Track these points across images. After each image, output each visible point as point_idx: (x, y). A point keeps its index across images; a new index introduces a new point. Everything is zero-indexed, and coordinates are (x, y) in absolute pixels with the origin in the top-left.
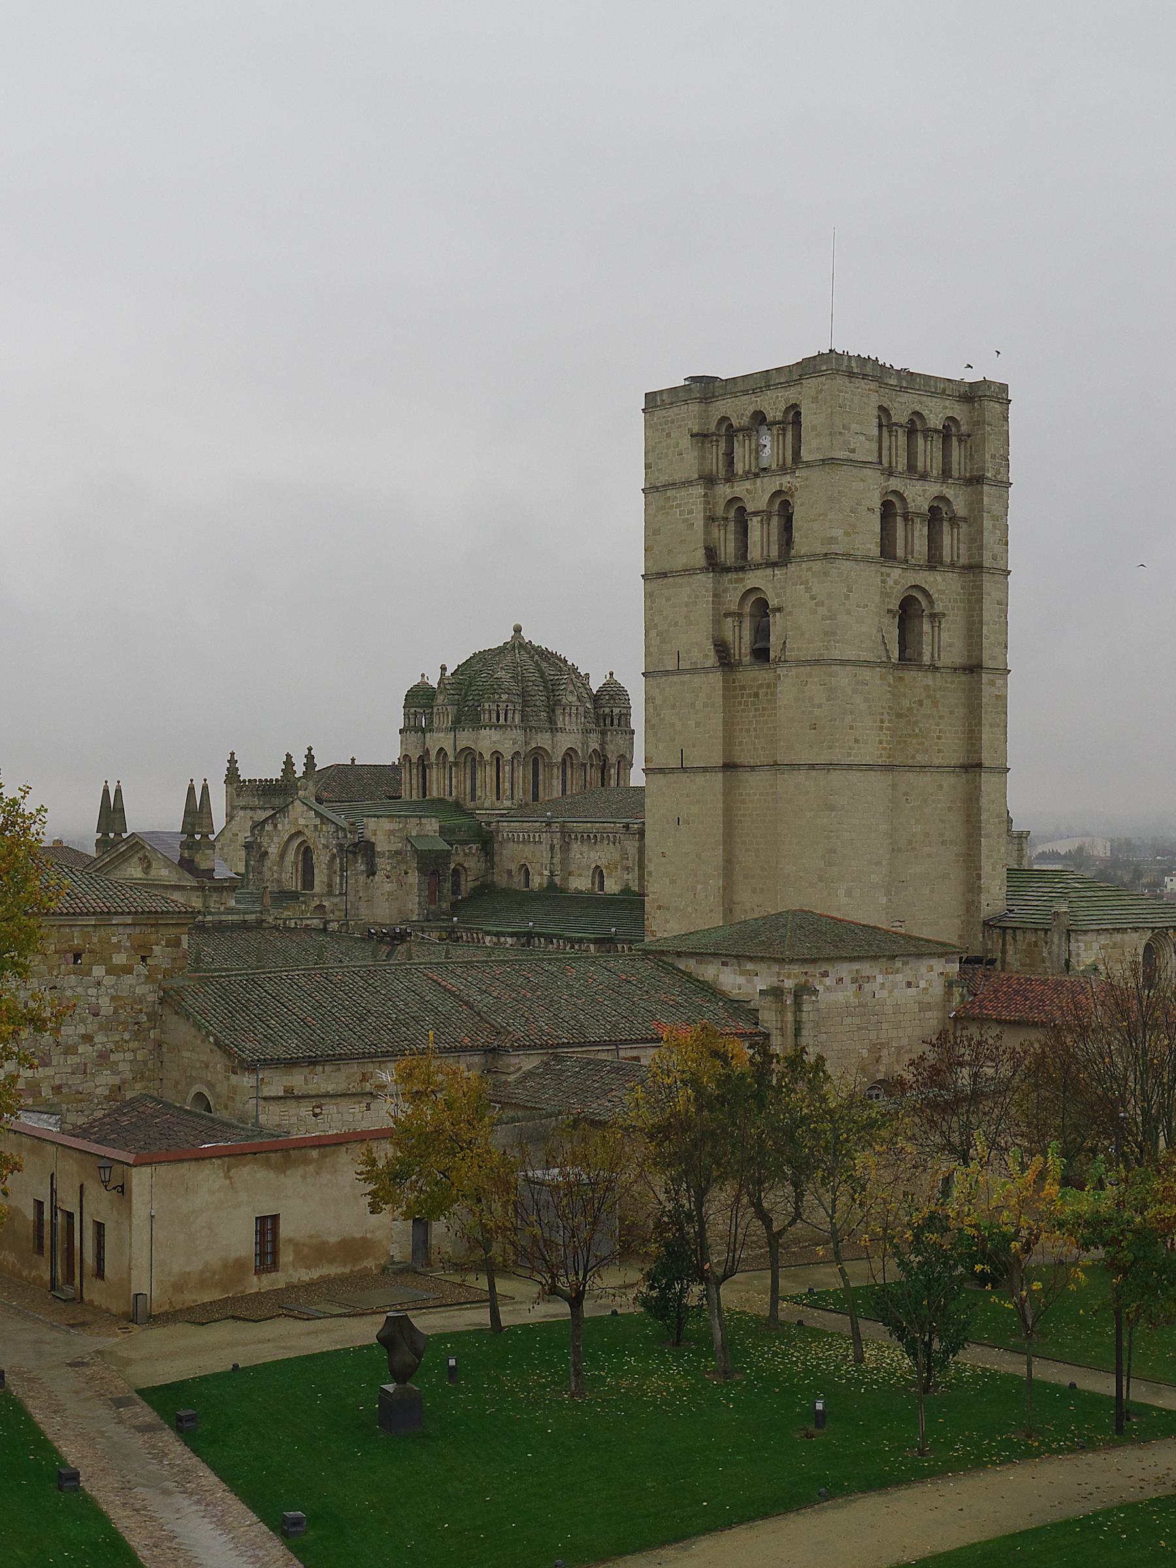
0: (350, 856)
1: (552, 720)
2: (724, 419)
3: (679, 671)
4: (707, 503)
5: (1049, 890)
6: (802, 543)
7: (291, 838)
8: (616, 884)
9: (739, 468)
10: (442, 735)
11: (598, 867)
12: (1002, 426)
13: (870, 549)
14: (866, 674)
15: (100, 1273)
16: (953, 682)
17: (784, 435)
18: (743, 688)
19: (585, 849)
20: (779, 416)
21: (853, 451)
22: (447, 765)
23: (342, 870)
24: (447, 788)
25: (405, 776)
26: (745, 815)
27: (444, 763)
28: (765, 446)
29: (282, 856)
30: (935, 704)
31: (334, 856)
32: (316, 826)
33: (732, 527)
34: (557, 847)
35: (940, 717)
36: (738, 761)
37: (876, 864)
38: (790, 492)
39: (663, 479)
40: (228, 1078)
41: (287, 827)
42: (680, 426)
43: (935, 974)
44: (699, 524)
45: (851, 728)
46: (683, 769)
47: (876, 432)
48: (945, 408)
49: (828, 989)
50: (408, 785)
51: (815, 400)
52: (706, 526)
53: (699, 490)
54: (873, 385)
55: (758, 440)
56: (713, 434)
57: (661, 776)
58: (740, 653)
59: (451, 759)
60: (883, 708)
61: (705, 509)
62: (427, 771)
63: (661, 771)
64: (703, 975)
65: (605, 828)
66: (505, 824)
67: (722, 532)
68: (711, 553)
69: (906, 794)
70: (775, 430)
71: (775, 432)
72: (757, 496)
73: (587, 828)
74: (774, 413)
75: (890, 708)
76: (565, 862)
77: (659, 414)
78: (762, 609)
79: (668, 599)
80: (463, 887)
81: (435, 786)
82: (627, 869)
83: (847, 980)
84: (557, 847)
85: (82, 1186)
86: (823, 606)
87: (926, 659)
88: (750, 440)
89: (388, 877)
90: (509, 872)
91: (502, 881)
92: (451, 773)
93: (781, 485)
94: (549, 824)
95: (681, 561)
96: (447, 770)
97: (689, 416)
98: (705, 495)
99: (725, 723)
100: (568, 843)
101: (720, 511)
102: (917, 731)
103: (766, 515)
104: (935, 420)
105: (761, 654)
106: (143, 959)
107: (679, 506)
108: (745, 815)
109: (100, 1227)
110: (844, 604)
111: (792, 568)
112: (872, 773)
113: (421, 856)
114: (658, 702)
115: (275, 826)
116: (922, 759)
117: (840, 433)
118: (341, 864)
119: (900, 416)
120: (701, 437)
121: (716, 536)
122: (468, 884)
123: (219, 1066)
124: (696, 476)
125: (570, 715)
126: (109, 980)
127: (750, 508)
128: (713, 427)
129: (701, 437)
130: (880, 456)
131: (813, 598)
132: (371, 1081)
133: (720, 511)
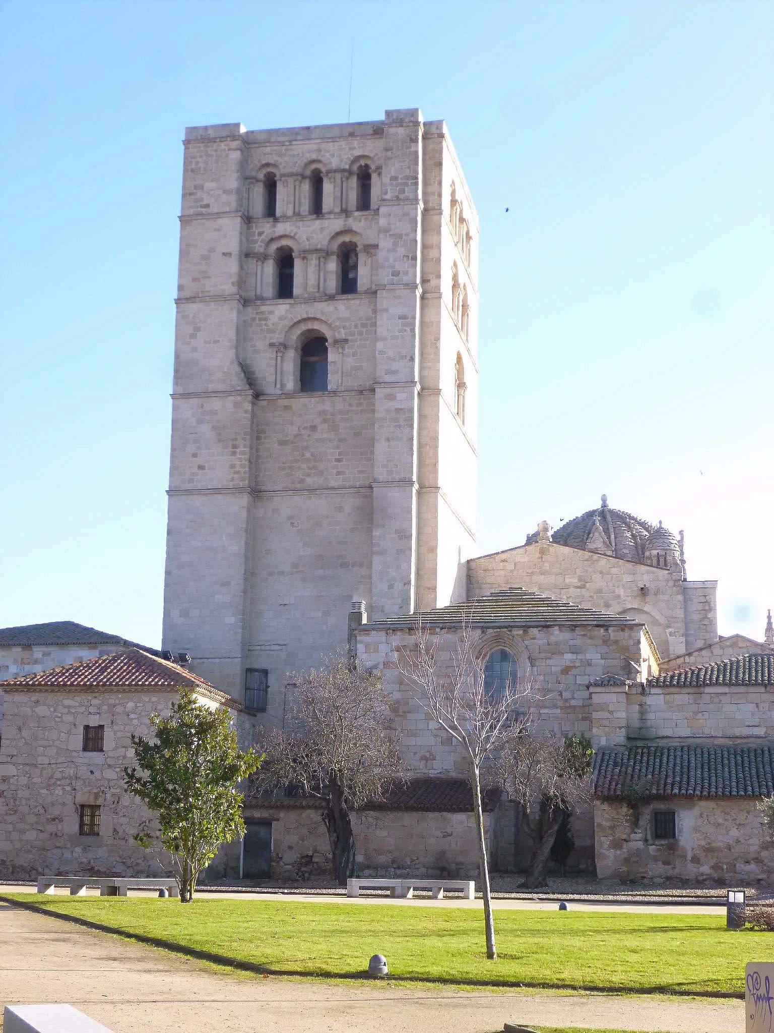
12: (410, 147)
13: (224, 290)
14: (216, 404)
16: (359, 405)
21: (207, 206)
30: (334, 428)
37: (223, 585)
45: (194, 455)
69: (290, 518)
110: (189, 343)
112: (220, 497)
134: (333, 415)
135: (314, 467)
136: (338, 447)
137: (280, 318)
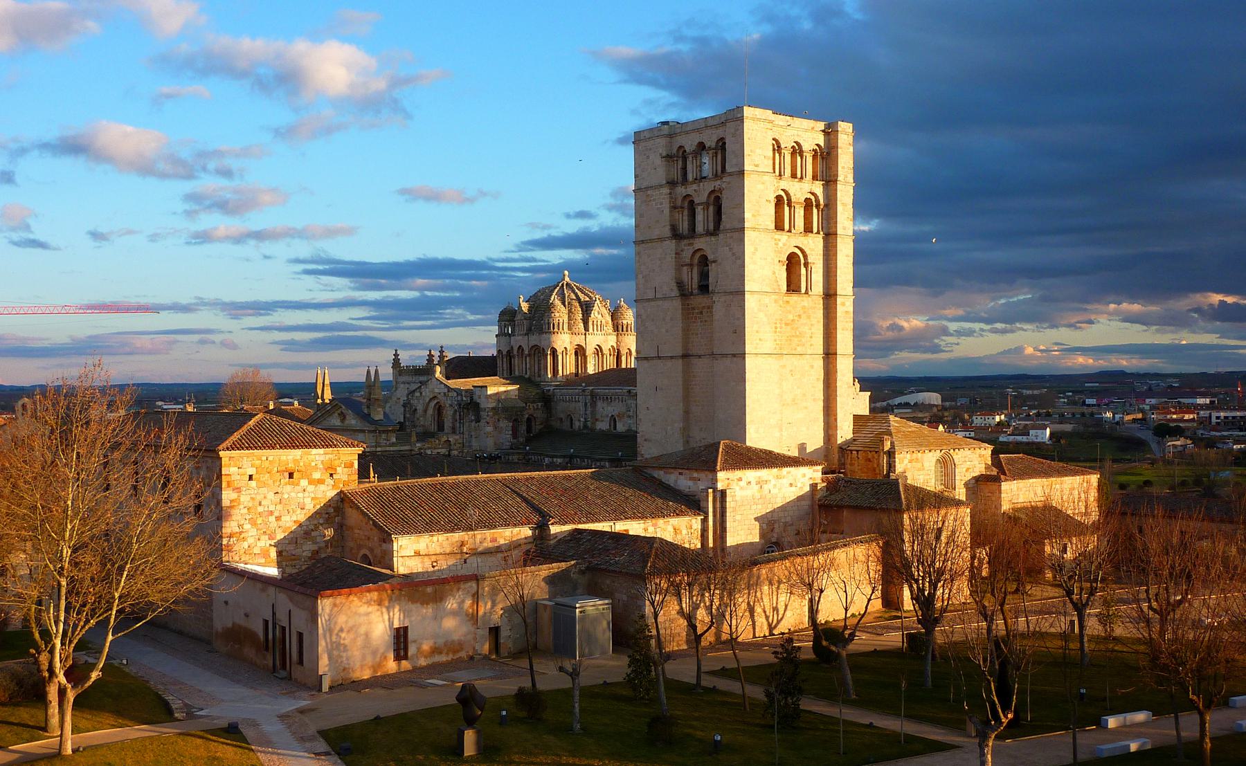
0: (465, 411)
1: (586, 329)
2: (681, 147)
3: (655, 299)
4: (671, 198)
5: (879, 427)
6: (726, 222)
7: (431, 400)
8: (624, 425)
9: (690, 177)
10: (520, 337)
11: (612, 416)
13: (767, 225)
14: (767, 300)
15: (301, 662)
17: (716, 157)
18: (693, 309)
19: (605, 405)
20: (713, 145)
21: (757, 166)
22: (524, 356)
23: (460, 419)
24: (524, 370)
25: (499, 362)
26: (695, 385)
27: (522, 355)
28: (705, 163)
29: (425, 411)
30: (809, 317)
31: (456, 411)
32: (445, 393)
33: (686, 212)
34: (589, 404)
35: (812, 325)
36: (690, 353)
38: (720, 190)
39: (645, 185)
40: (380, 546)
41: (428, 394)
42: (655, 152)
43: (807, 478)
44: (667, 211)
45: (757, 332)
46: (659, 358)
47: (771, 154)
48: (814, 138)
49: (742, 488)
50: (501, 369)
51: (734, 135)
52: (671, 212)
53: (666, 190)
54: (770, 126)
55: (701, 159)
56: (674, 156)
57: (645, 361)
58: (692, 288)
59: (526, 352)
60: (776, 320)
61: (670, 201)
62: (513, 360)
63: (646, 358)
64: (668, 481)
65: (616, 393)
66: (558, 391)
67: (681, 215)
68: (674, 228)
69: (791, 371)
70: (711, 152)
71: (711, 155)
72: (701, 193)
73: (606, 393)
74: (710, 141)
75: (781, 320)
76: (593, 413)
77: (643, 144)
78: (704, 261)
79: (649, 256)
80: (533, 428)
81: (517, 368)
82: (629, 417)
83: (753, 482)
84: (589, 404)
85: (290, 611)
86: (739, 259)
87: (803, 290)
88: (696, 160)
89: (488, 423)
90: (561, 419)
91: (556, 424)
92: (526, 361)
93: (715, 186)
94: (584, 391)
95: (656, 233)
96: (524, 358)
97: (661, 147)
98: (670, 194)
99: (683, 330)
100: (595, 402)
101: (679, 203)
102: (798, 333)
103: (707, 204)
104: (808, 146)
105: (704, 288)
106: (331, 475)
107: (654, 200)
108: (695, 385)
109: (300, 635)
111: (721, 236)
113: (505, 409)
114: (644, 317)
115: (421, 393)
116: (799, 350)
117: (749, 155)
118: (460, 415)
119: (787, 144)
120: (669, 157)
121: (677, 218)
122: (537, 427)
123: (376, 538)
124: (664, 182)
125: (597, 325)
126: (311, 488)
127: (697, 201)
128: (675, 151)
129: (669, 157)
130: (774, 169)
131: (734, 254)
132: (467, 546)
133: (679, 203)
134: (808, 309)
135: (800, 341)
136: (810, 329)
137: (784, 245)
